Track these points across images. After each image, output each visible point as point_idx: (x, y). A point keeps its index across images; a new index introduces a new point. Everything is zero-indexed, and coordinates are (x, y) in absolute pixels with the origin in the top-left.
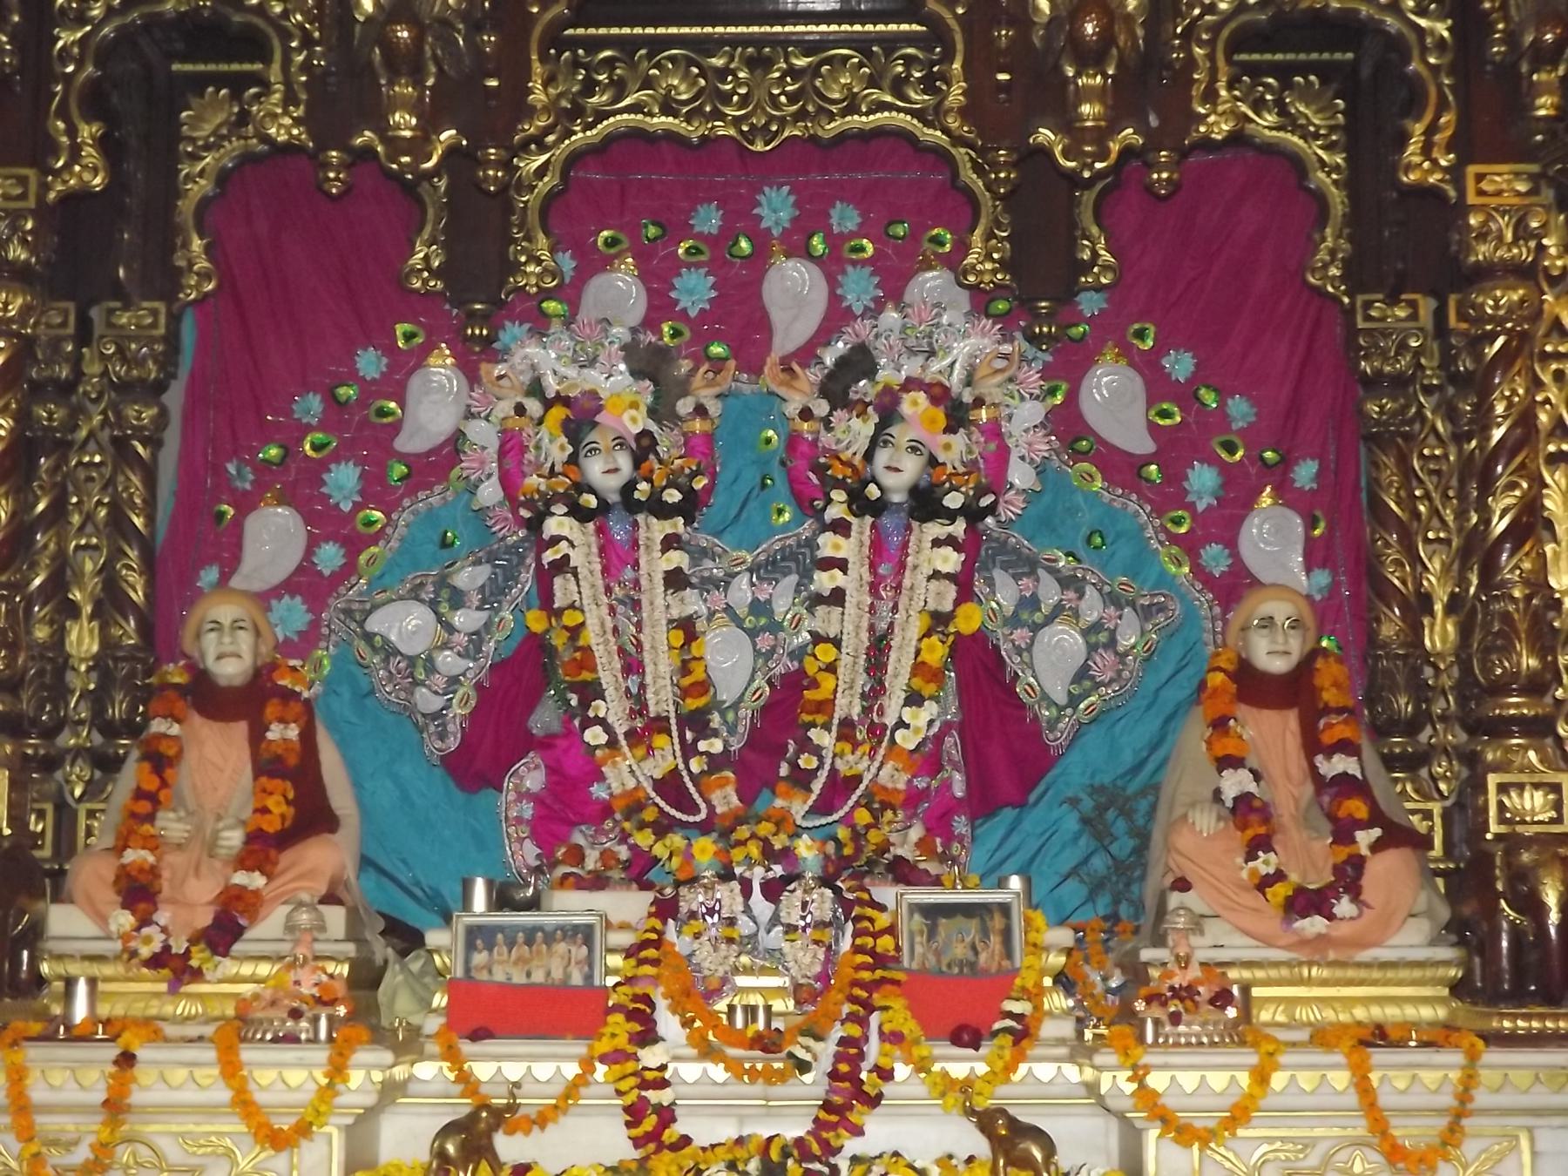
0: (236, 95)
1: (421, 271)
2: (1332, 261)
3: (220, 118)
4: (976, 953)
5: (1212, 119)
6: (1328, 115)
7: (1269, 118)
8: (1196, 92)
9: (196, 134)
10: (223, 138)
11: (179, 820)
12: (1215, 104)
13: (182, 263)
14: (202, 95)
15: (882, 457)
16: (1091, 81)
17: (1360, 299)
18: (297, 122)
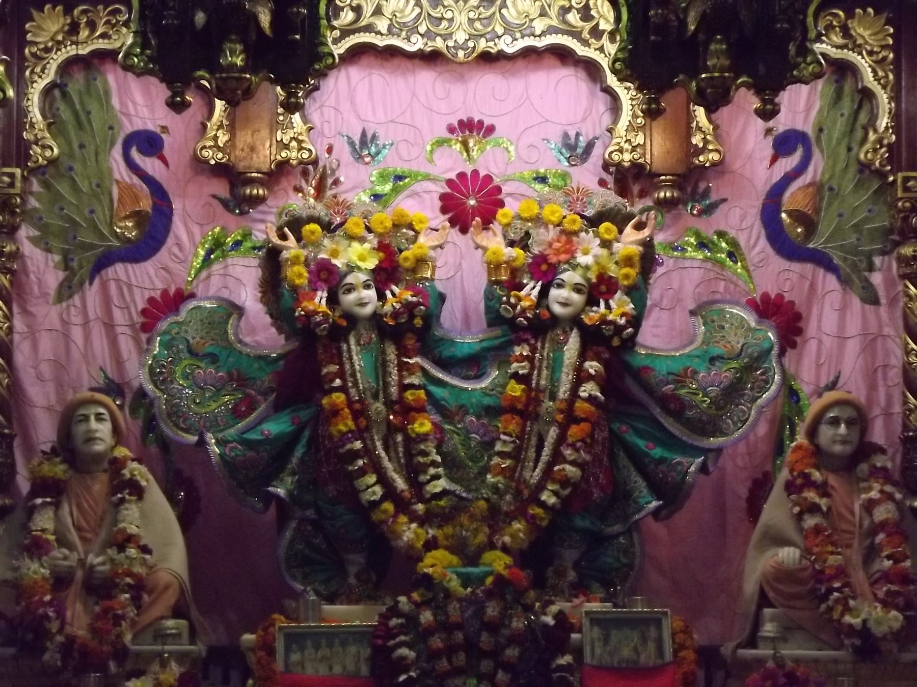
0: (68, 11)
1: (210, 147)
2: (881, 148)
3: (54, 28)
4: (638, 654)
5: (803, 65)
6: (880, 36)
7: (834, 38)
8: (792, 48)
9: (38, 40)
10: (59, 43)
11: (65, 558)
12: (805, 57)
13: (32, 138)
14: (43, 12)
15: (554, 292)
16: (718, 46)
17: (900, 175)
18: (151, 59)
